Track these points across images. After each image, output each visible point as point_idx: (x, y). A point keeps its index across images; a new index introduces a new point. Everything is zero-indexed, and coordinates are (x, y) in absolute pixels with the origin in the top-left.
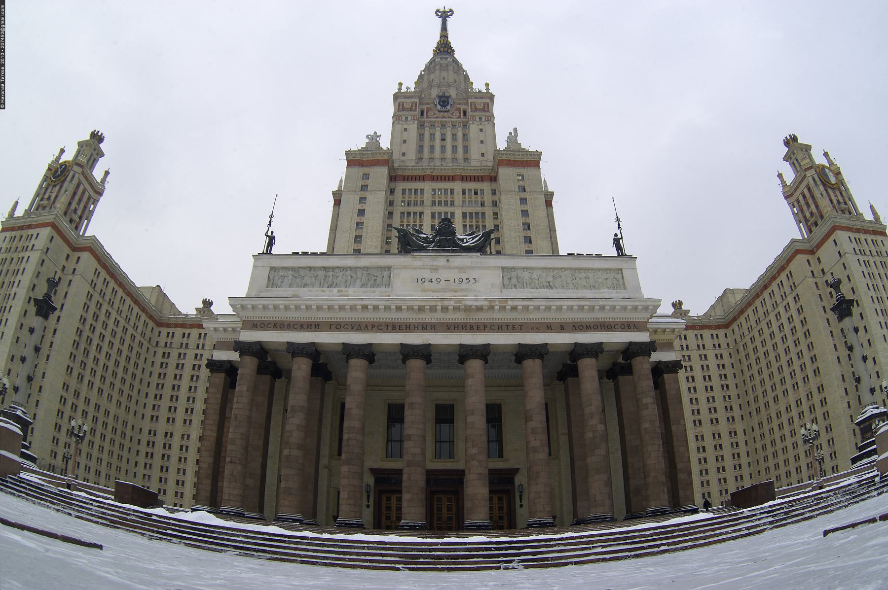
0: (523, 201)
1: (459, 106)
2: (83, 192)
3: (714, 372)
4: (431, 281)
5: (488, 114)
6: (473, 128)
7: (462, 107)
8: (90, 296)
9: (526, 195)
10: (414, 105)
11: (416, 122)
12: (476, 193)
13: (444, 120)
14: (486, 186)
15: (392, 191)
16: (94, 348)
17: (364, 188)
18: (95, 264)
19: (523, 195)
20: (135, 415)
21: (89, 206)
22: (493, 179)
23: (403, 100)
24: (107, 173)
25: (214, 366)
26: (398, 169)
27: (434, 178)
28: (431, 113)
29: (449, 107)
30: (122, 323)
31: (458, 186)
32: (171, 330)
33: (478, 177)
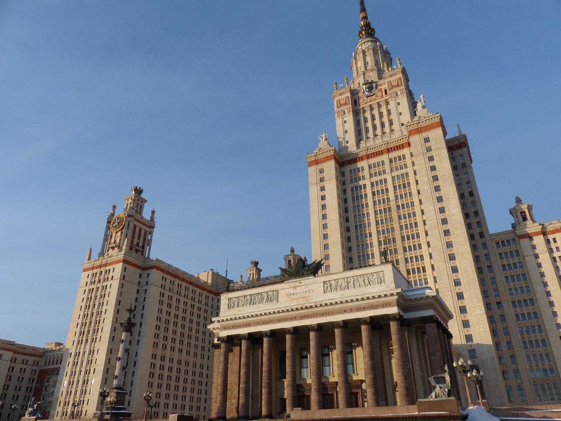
1: (380, 87)
2: (140, 231)
4: (294, 294)
8: (162, 295)
10: (347, 100)
11: (351, 113)
12: (400, 159)
14: (406, 151)
15: (343, 174)
16: (172, 325)
18: (161, 274)
20: (208, 359)
21: (147, 237)
23: (340, 98)
24: (153, 212)
26: (343, 157)
29: (373, 91)
30: (190, 302)
31: (385, 158)
33: (399, 146)
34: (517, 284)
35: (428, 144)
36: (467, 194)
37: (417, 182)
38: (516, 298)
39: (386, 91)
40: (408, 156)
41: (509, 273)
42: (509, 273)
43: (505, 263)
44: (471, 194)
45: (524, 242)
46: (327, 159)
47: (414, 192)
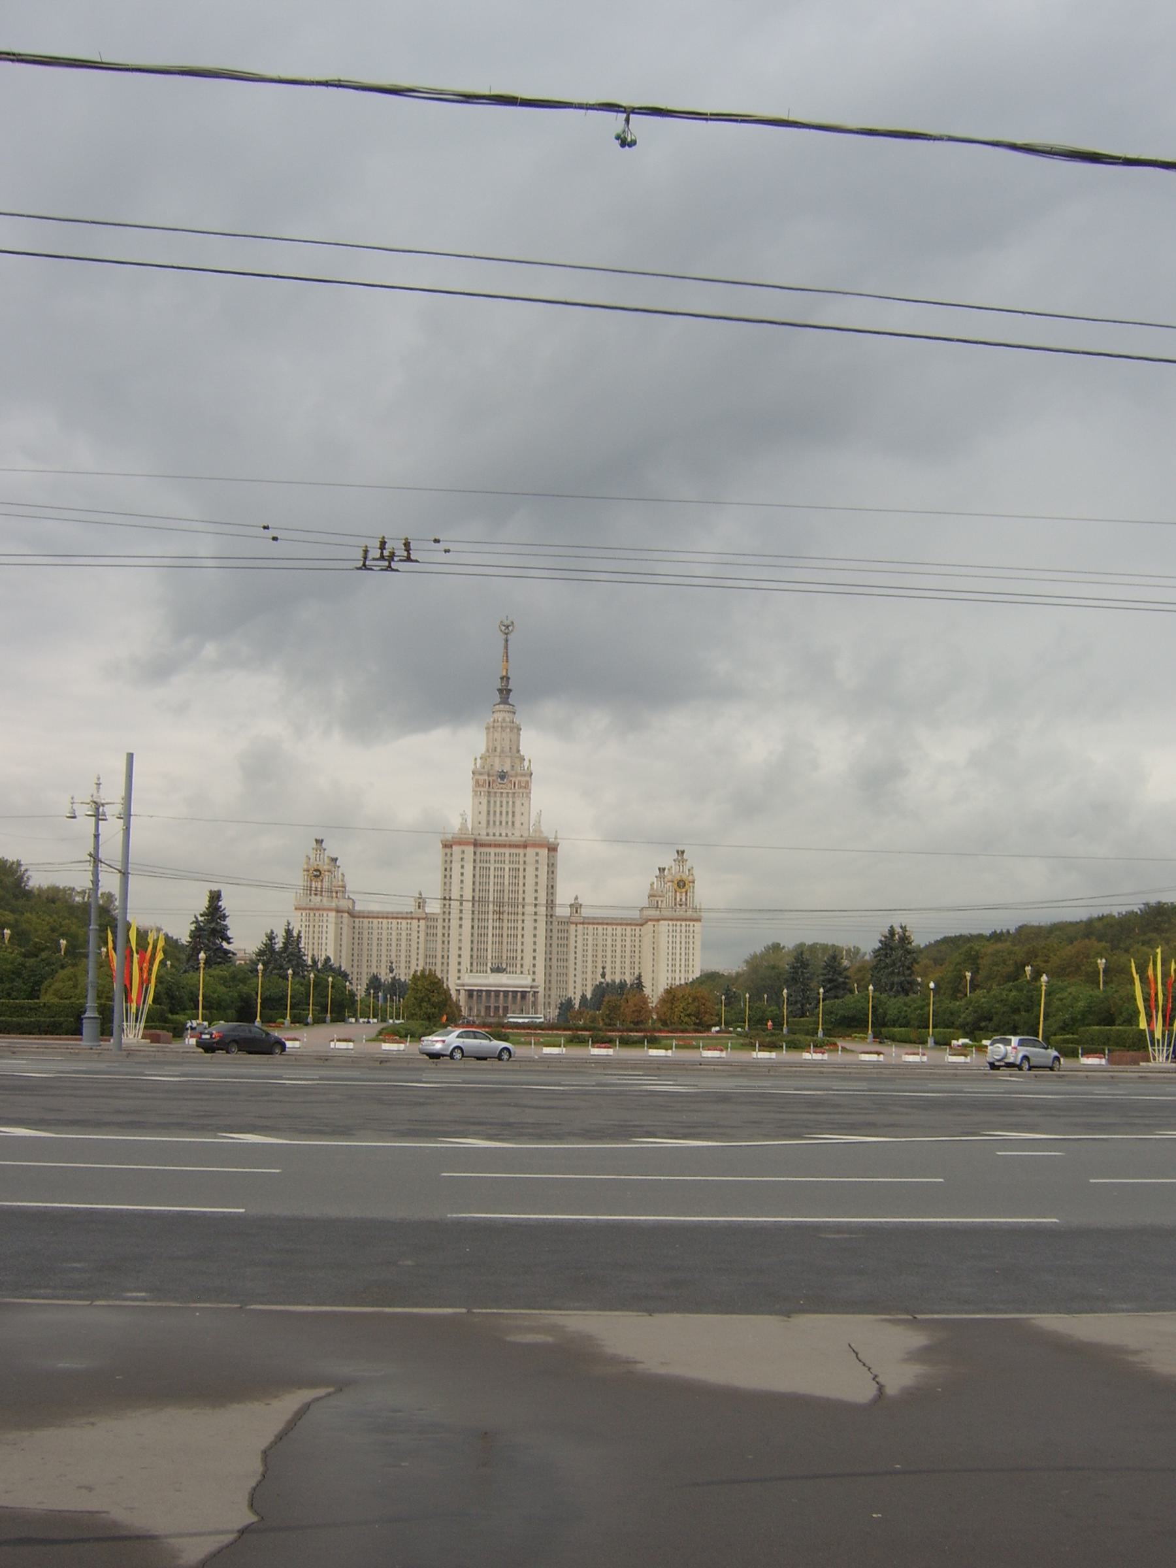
0: (537, 869)
3: (628, 949)
5: (528, 791)
6: (518, 803)
7: (513, 779)
9: (539, 866)
13: (502, 791)
14: (521, 851)
17: (462, 859)
19: (537, 866)
22: (525, 846)
25: (457, 990)
27: (496, 846)
28: (494, 785)
31: (507, 851)
32: (361, 920)
34: (562, 949)
35: (537, 858)
36: (550, 887)
37: (524, 877)
38: (559, 957)
39: (515, 783)
40: (522, 855)
41: (560, 942)
42: (560, 942)
43: (560, 936)
44: (552, 887)
45: (573, 927)
46: (467, 843)
47: (521, 884)
